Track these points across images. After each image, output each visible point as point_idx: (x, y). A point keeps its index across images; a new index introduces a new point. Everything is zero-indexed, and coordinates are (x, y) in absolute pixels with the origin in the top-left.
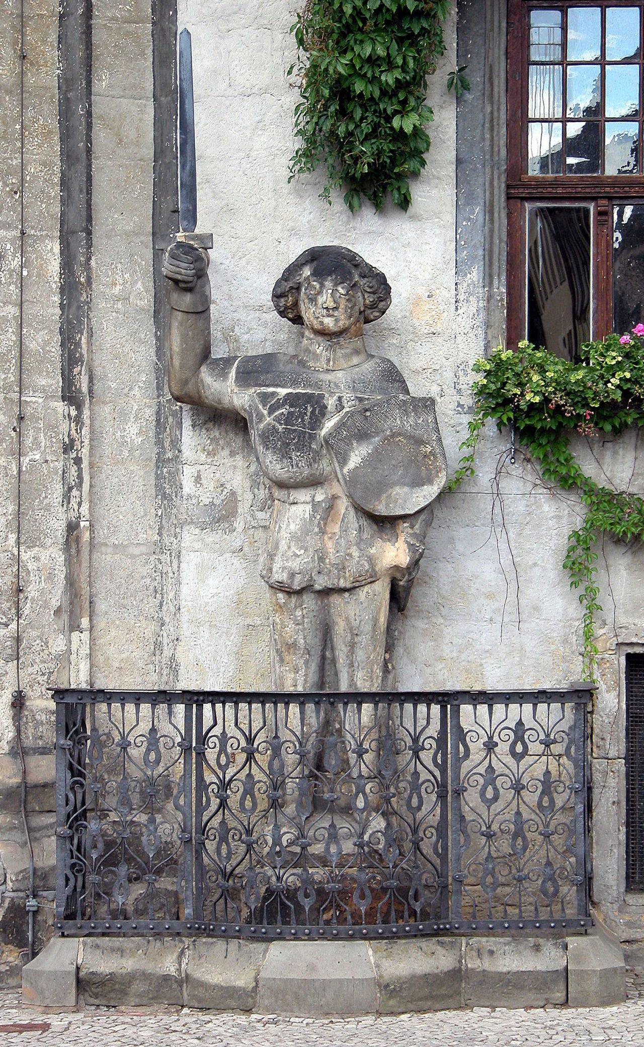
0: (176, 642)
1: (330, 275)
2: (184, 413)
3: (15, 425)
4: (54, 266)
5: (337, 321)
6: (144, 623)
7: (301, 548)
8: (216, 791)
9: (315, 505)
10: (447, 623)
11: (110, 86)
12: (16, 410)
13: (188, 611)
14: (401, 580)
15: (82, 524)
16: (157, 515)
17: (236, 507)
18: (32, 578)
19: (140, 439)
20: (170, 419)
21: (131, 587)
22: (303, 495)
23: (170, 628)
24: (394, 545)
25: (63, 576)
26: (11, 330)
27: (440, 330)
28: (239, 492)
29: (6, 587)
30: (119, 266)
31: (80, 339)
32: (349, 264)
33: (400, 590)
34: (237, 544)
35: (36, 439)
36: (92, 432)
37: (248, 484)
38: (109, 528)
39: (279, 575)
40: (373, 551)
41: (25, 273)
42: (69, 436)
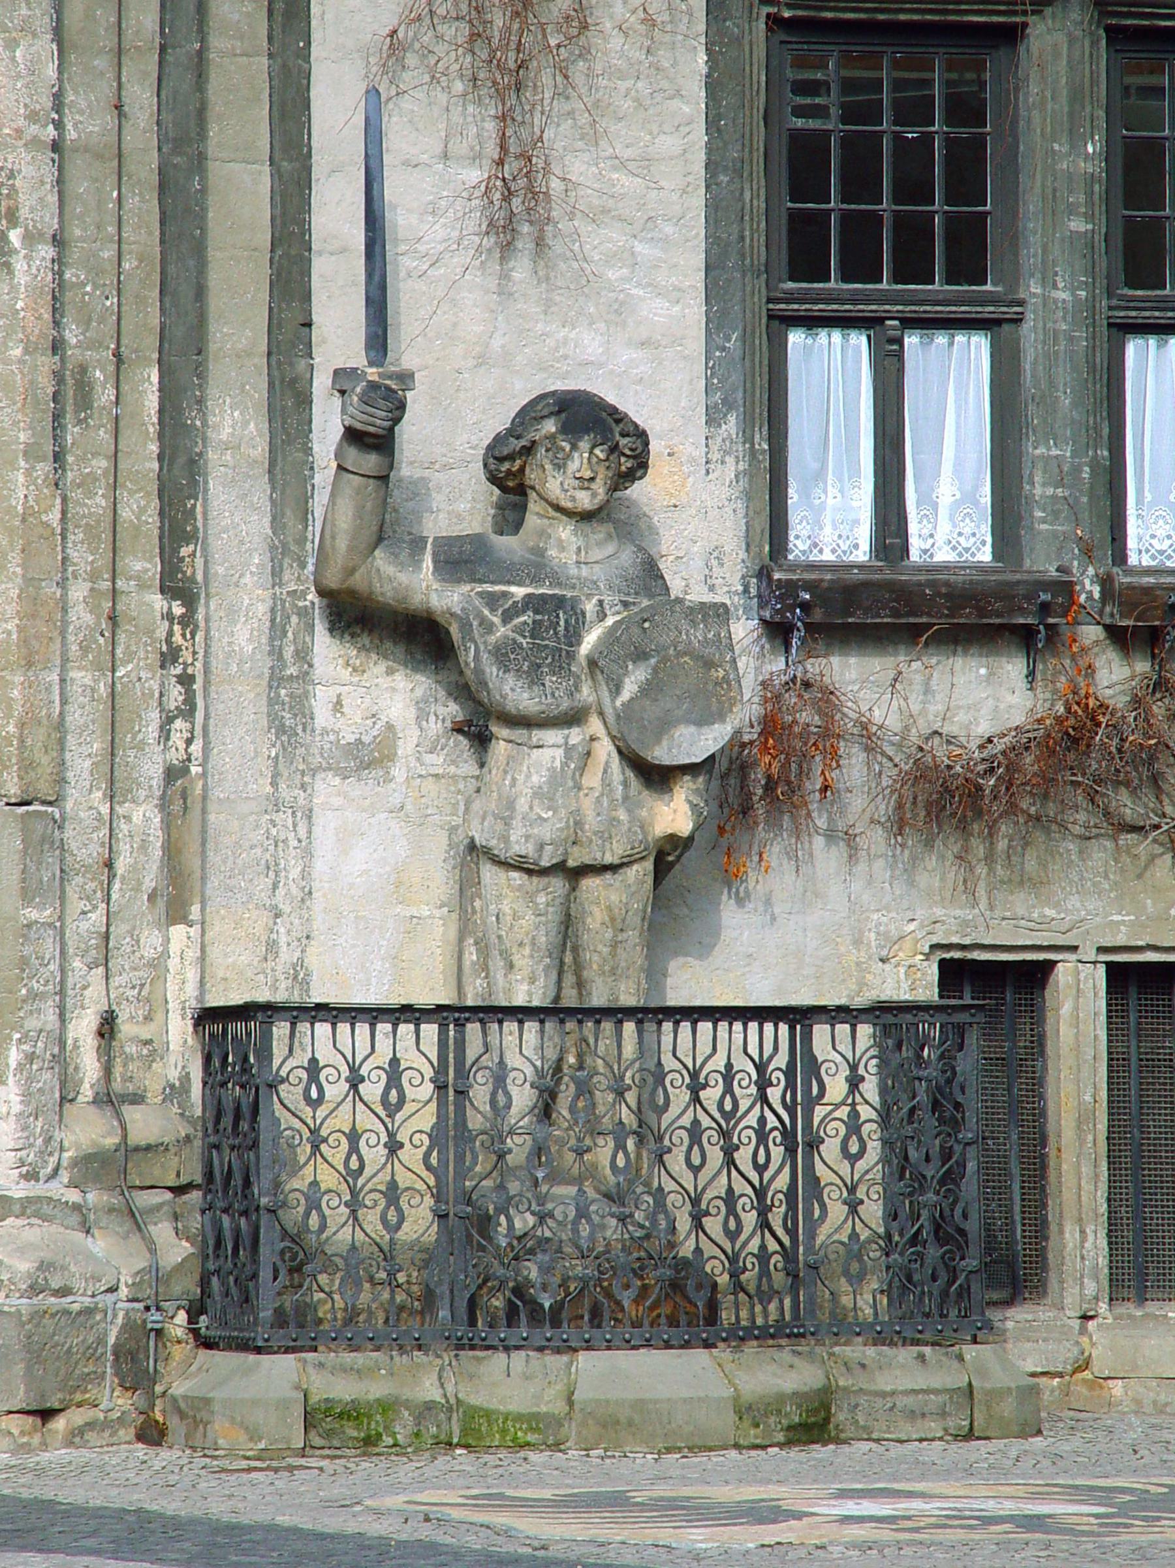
0: (304, 941)
1: (587, 432)
6: (255, 913)
7: (549, 809)
8: (487, 1144)
9: (569, 750)
14: (669, 854)
17: (395, 747)
19: (251, 647)
20: (294, 619)
22: (552, 736)
24: (668, 805)
25: (159, 844)
31: (194, 506)
34: (396, 800)
37: (412, 713)
40: (644, 813)
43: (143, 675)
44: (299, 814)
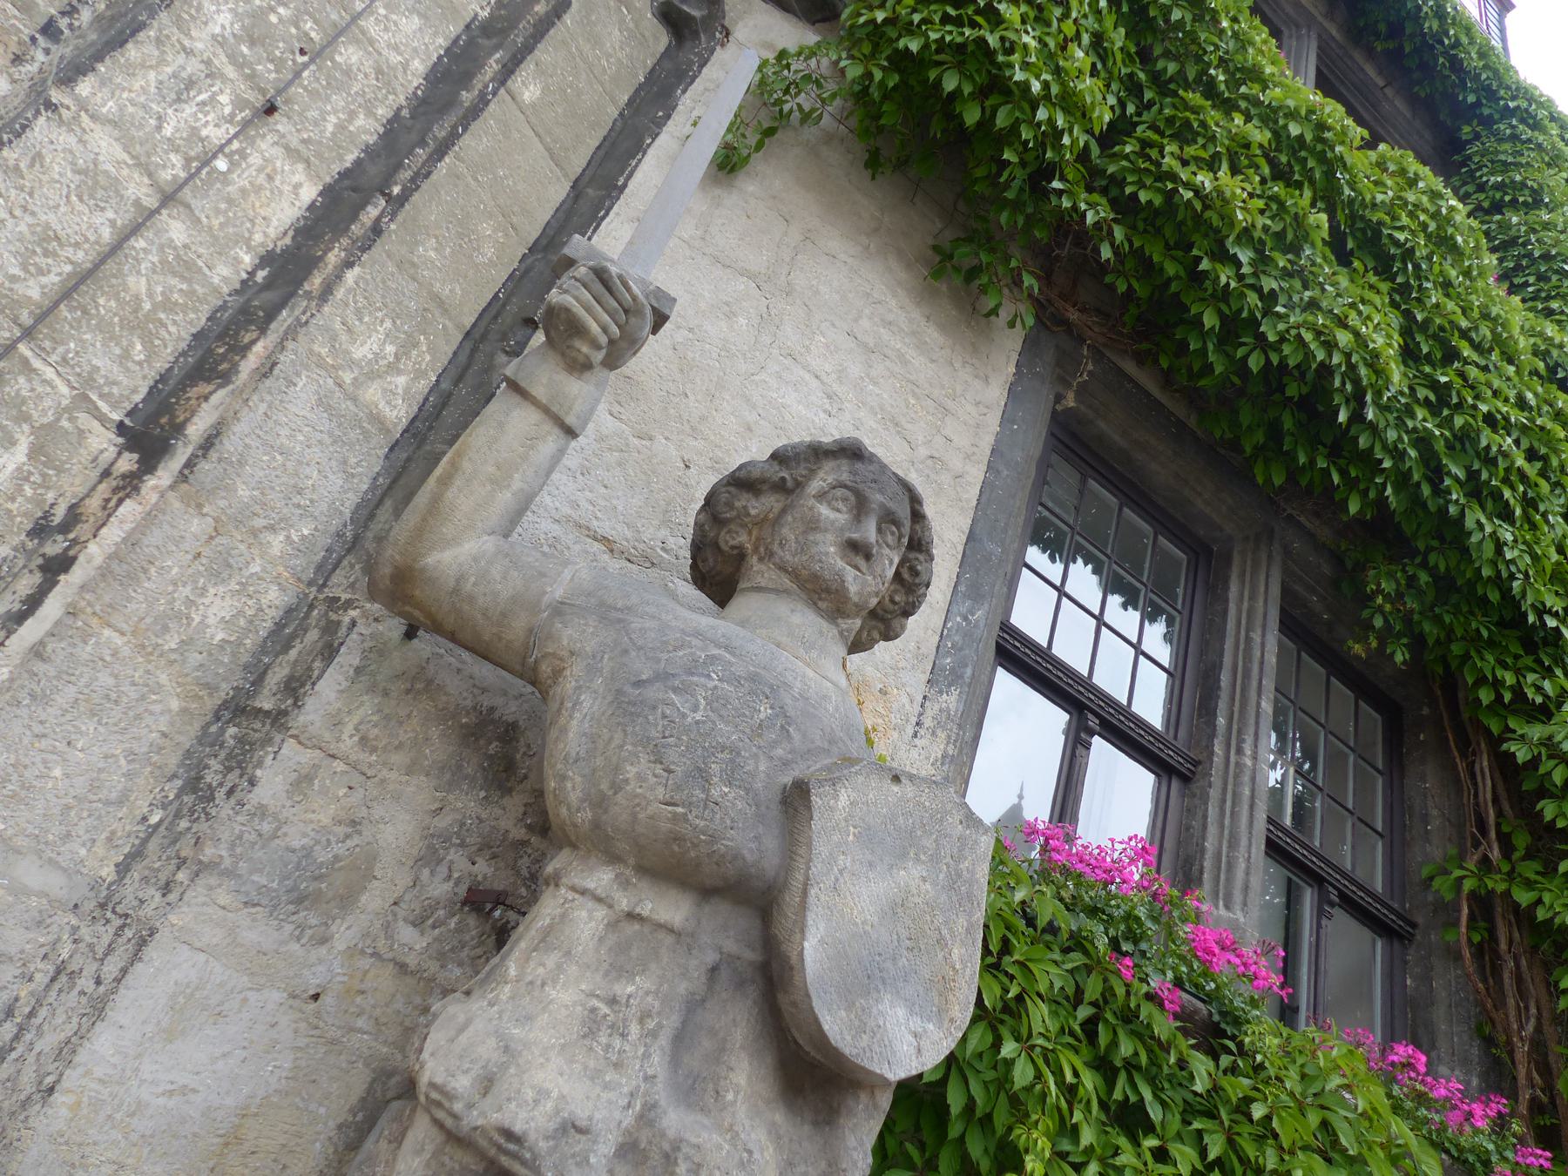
2: (354, 636)
11: (533, 105)
16: (145, 819)
19: (220, 636)
30: (388, 324)
36: (131, 542)
41: (221, 164)
42: (72, 507)
44: (129, 933)
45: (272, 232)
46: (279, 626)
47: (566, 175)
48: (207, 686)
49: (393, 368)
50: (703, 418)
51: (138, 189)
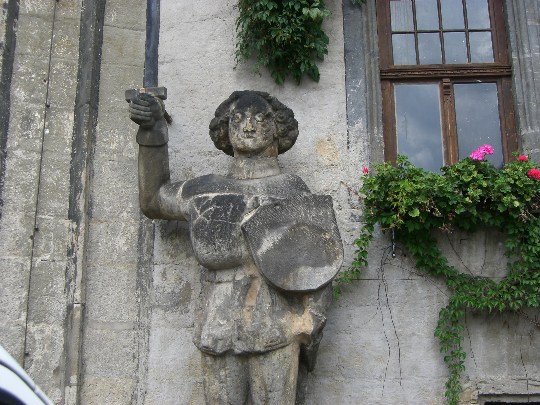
1: (249, 106)
2: (156, 228)
3: (32, 234)
4: (69, 129)
5: (255, 141)
6: (125, 380)
7: (224, 319)
9: (236, 283)
10: (347, 380)
11: (117, 21)
12: (33, 223)
13: (154, 371)
14: (308, 346)
15: (75, 305)
16: (137, 302)
18: (37, 345)
20: (147, 233)
21: (116, 354)
22: (226, 276)
23: (141, 384)
25: (62, 344)
26: (33, 169)
27: (337, 163)
28: (192, 283)
29: (16, 352)
30: (116, 131)
32: (264, 100)
33: (308, 354)
34: (190, 321)
35: (47, 245)
37: (198, 277)
38: (100, 310)
39: (207, 342)
40: (283, 321)
41: (47, 132)
43: (56, 258)
45: (70, 137)
46: (140, 236)
47: (142, 30)
48: (131, 262)
49: (126, 142)
50: (221, 87)
51: (36, 156)
